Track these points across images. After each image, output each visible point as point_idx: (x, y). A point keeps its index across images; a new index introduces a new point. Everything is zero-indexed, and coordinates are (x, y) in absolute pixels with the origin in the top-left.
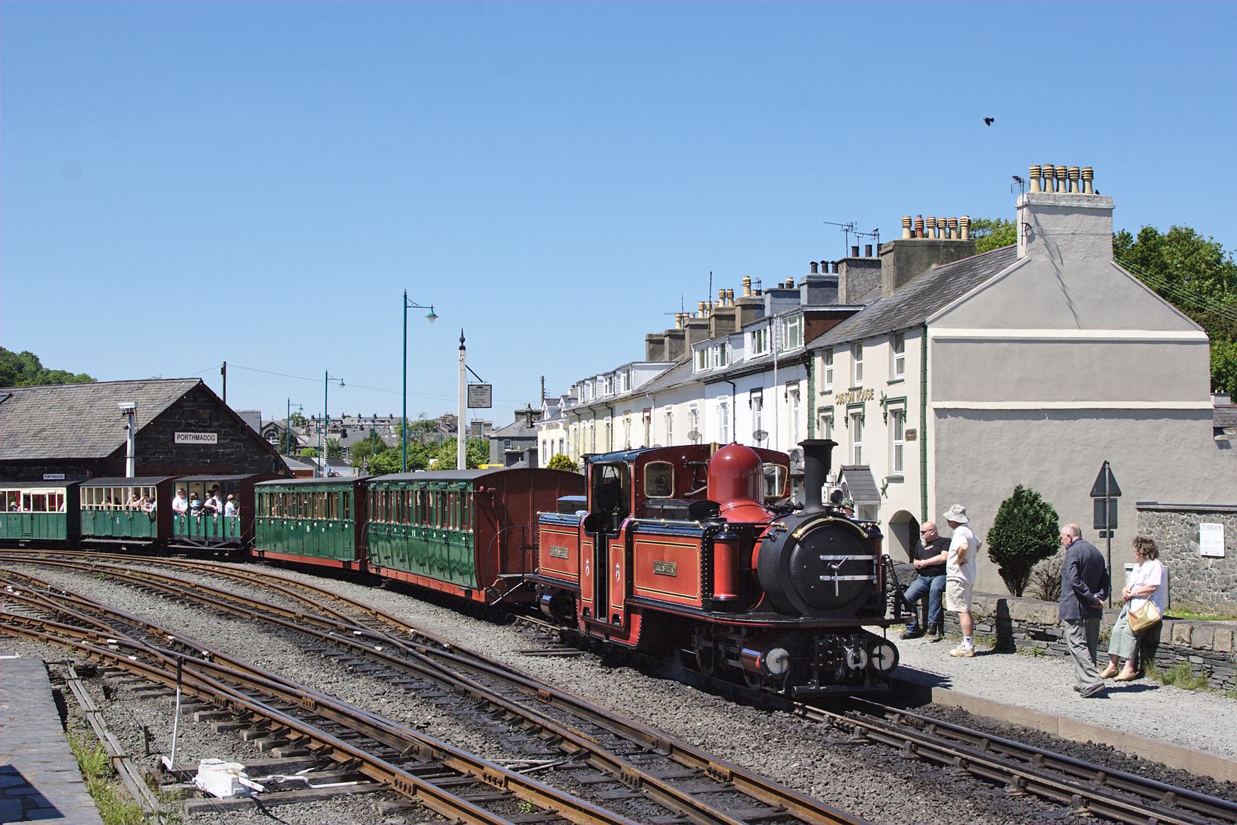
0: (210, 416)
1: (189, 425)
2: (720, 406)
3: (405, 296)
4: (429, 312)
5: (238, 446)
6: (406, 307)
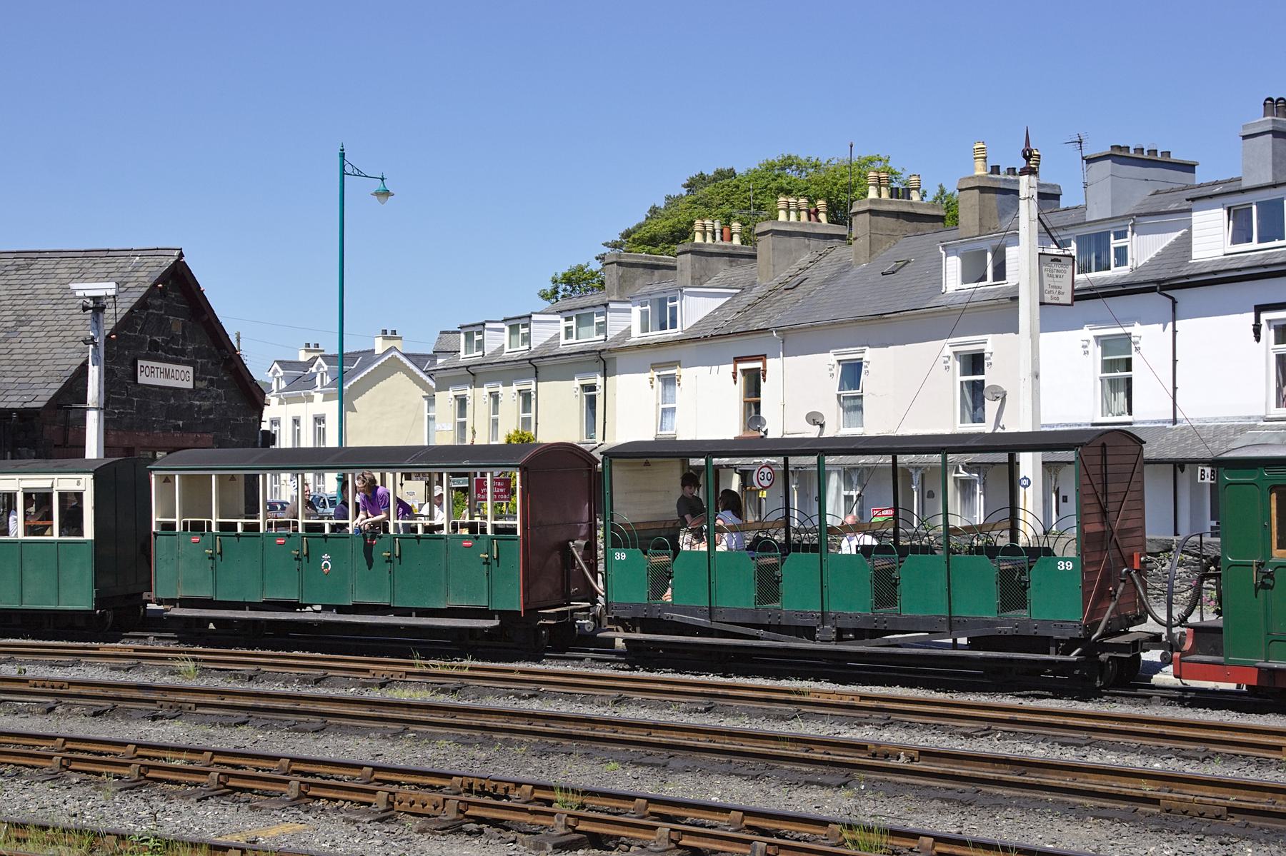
0: (183, 332)
1: (154, 346)
2: (1093, 340)
3: (343, 155)
4: (378, 185)
5: (218, 396)
6: (343, 173)
